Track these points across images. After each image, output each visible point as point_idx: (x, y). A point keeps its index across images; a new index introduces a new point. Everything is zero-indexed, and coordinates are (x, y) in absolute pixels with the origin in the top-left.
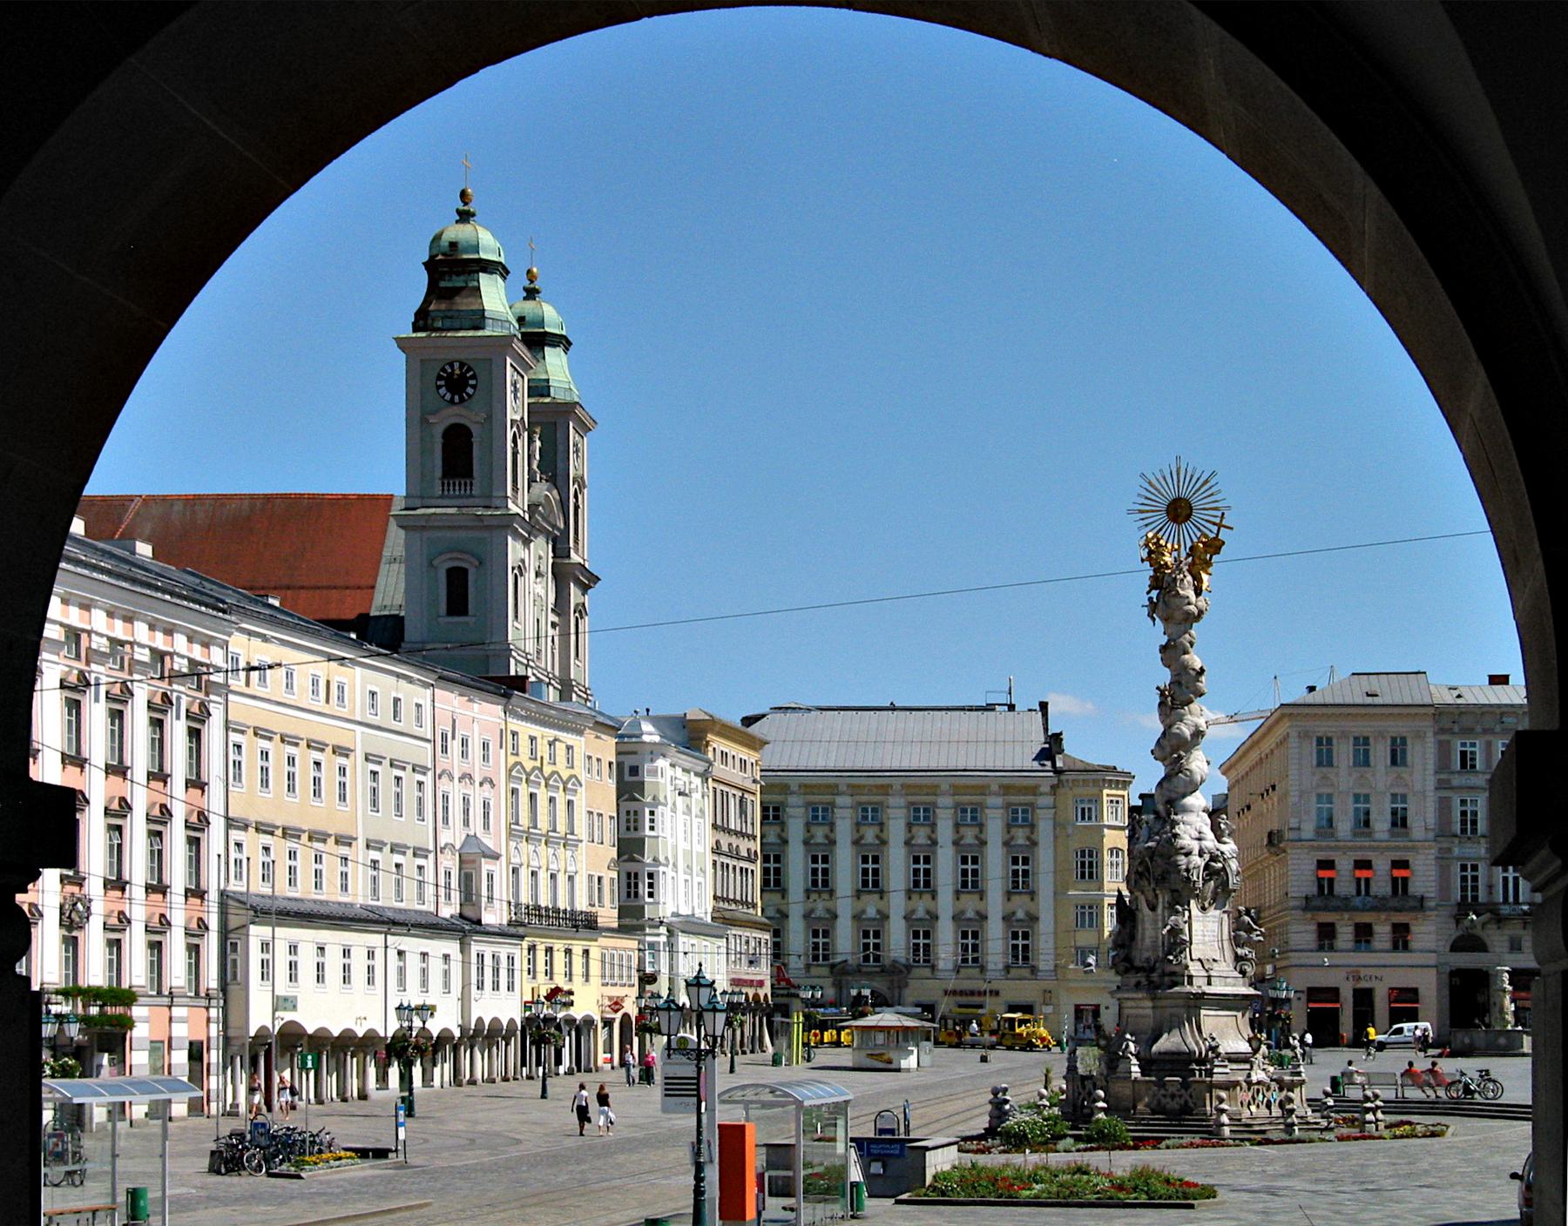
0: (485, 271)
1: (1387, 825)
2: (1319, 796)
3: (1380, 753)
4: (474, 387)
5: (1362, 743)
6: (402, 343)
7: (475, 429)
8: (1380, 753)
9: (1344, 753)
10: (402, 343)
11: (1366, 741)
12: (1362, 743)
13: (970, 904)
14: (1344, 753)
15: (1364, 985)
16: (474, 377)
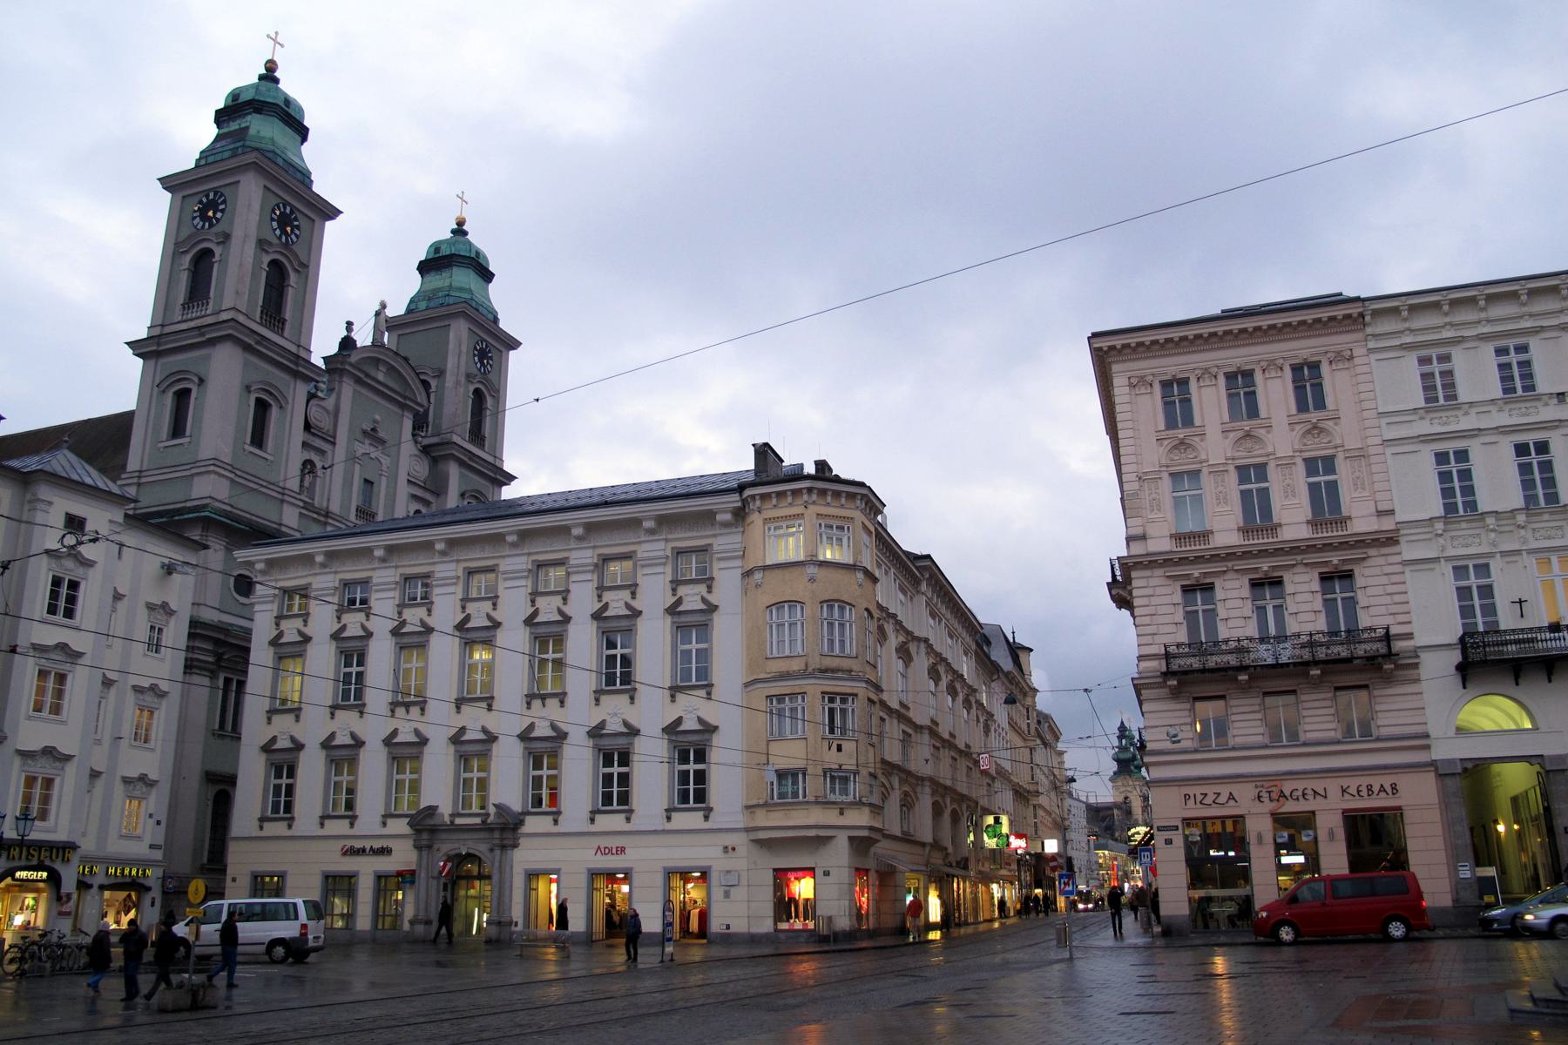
0: (258, 111)
1: (1305, 512)
2: (1176, 476)
3: (1276, 394)
4: (223, 211)
5: (1241, 384)
6: (169, 183)
7: (218, 250)
8: (1276, 394)
9: (1210, 402)
10: (169, 183)
11: (1248, 375)
12: (1241, 384)
13: (615, 711)
14: (1210, 402)
15: (1290, 807)
16: (224, 202)
